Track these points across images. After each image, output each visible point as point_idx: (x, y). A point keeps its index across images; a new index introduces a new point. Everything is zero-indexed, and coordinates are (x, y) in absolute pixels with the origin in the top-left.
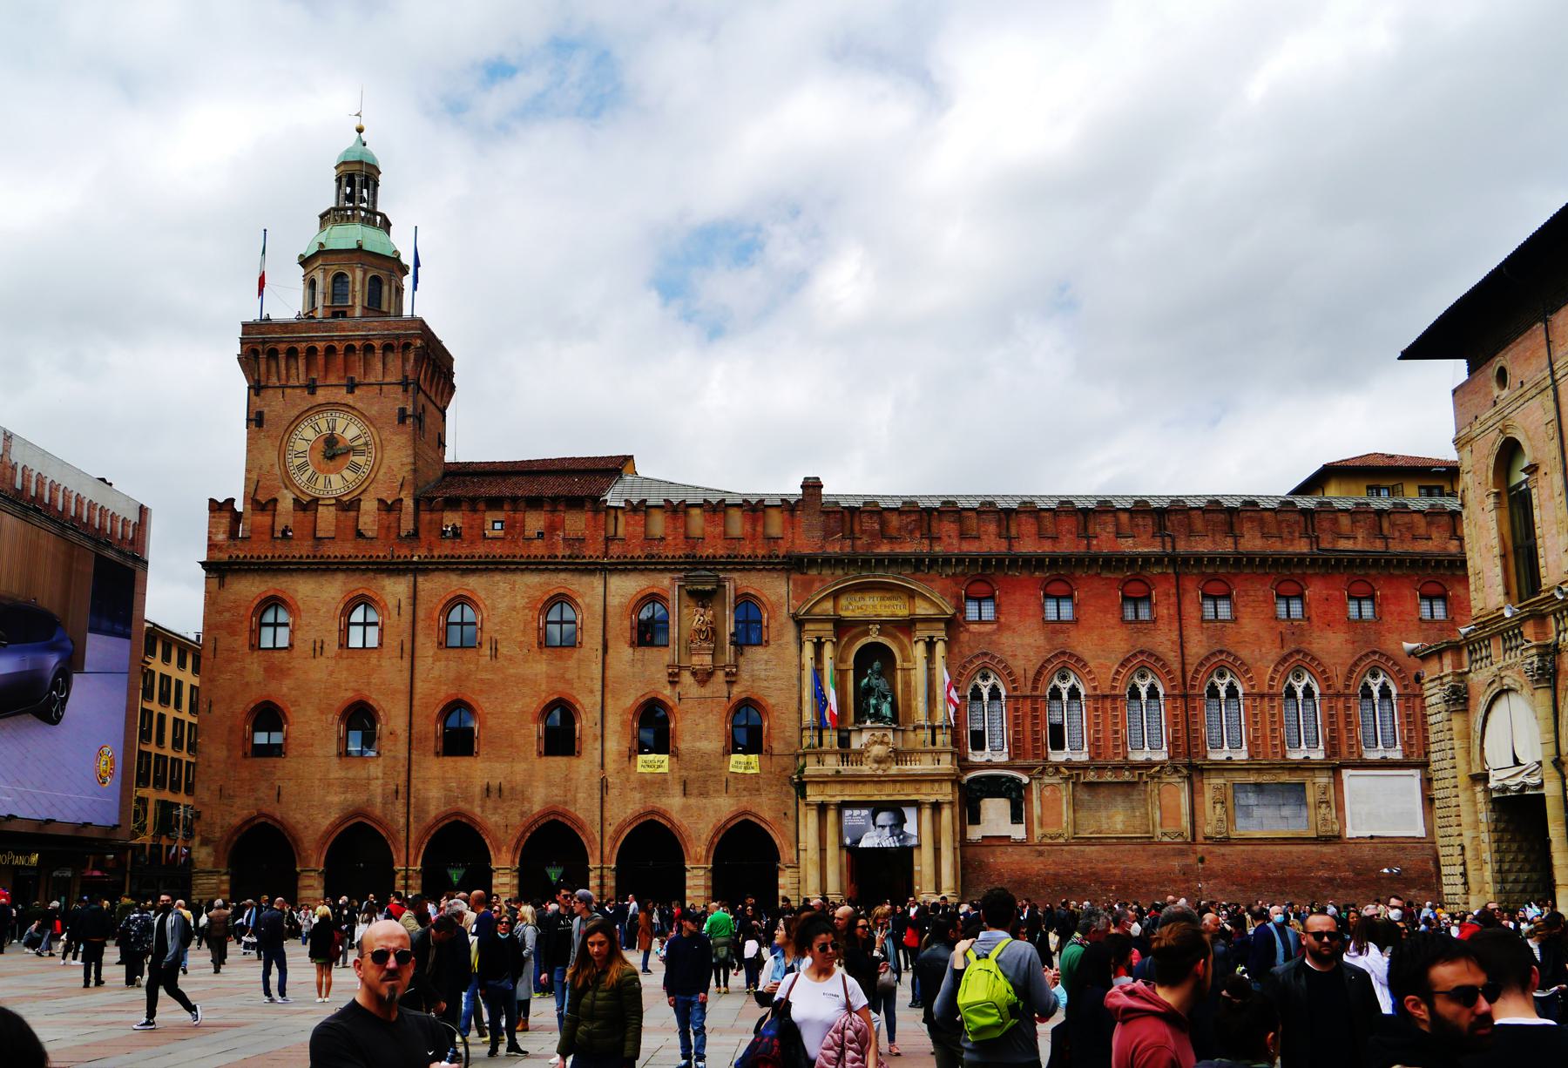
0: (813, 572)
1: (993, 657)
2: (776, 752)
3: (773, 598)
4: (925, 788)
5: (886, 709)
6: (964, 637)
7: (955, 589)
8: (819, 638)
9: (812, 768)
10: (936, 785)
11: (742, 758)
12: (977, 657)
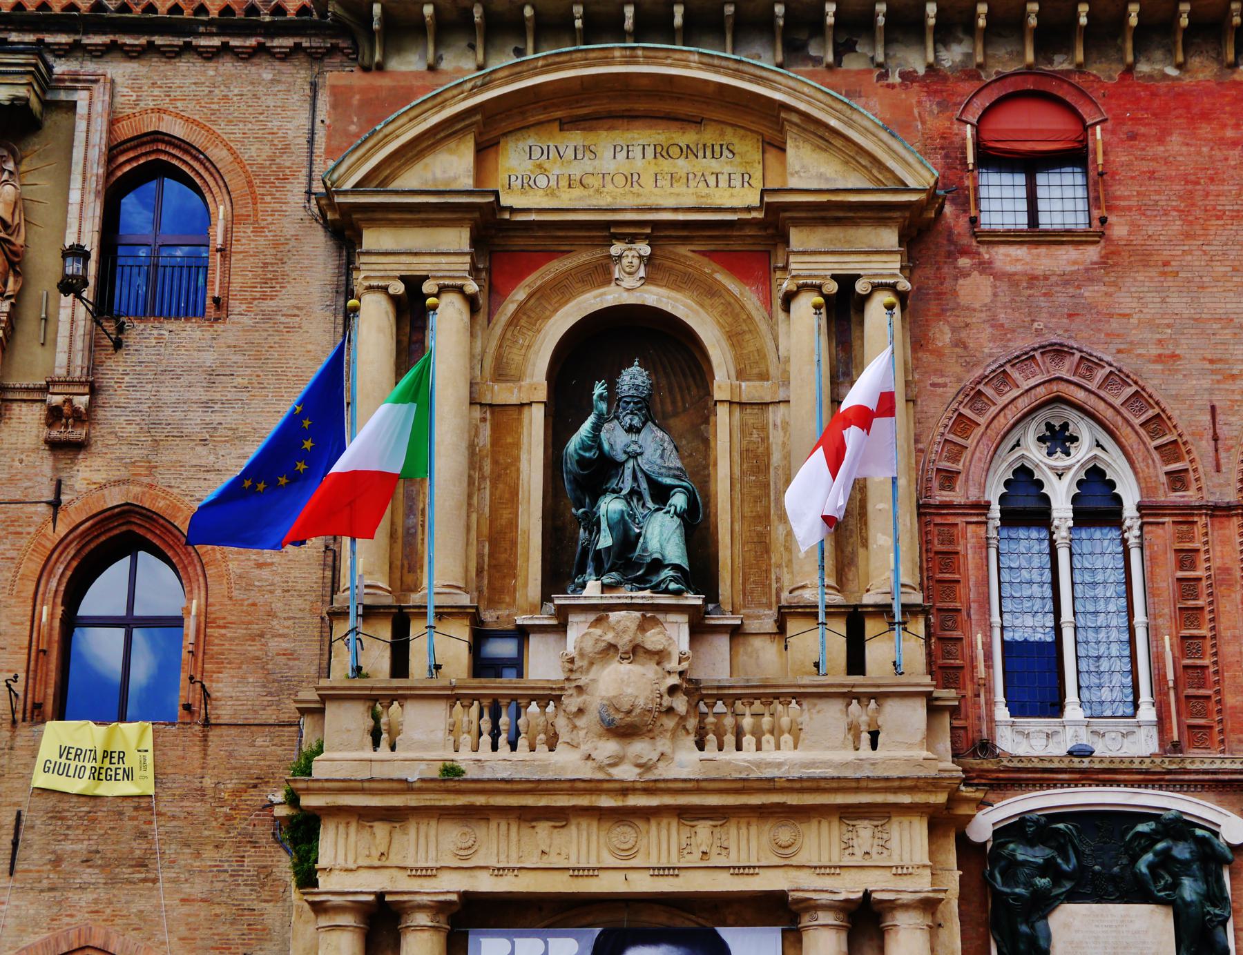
0: (409, 64)
1: (1088, 363)
2: (224, 712)
3: (254, 152)
4: (819, 842)
5: (662, 536)
6: (974, 290)
7: (937, 123)
8: (413, 283)
9: (343, 750)
10: (865, 831)
11: (83, 734)
12: (1025, 359)
